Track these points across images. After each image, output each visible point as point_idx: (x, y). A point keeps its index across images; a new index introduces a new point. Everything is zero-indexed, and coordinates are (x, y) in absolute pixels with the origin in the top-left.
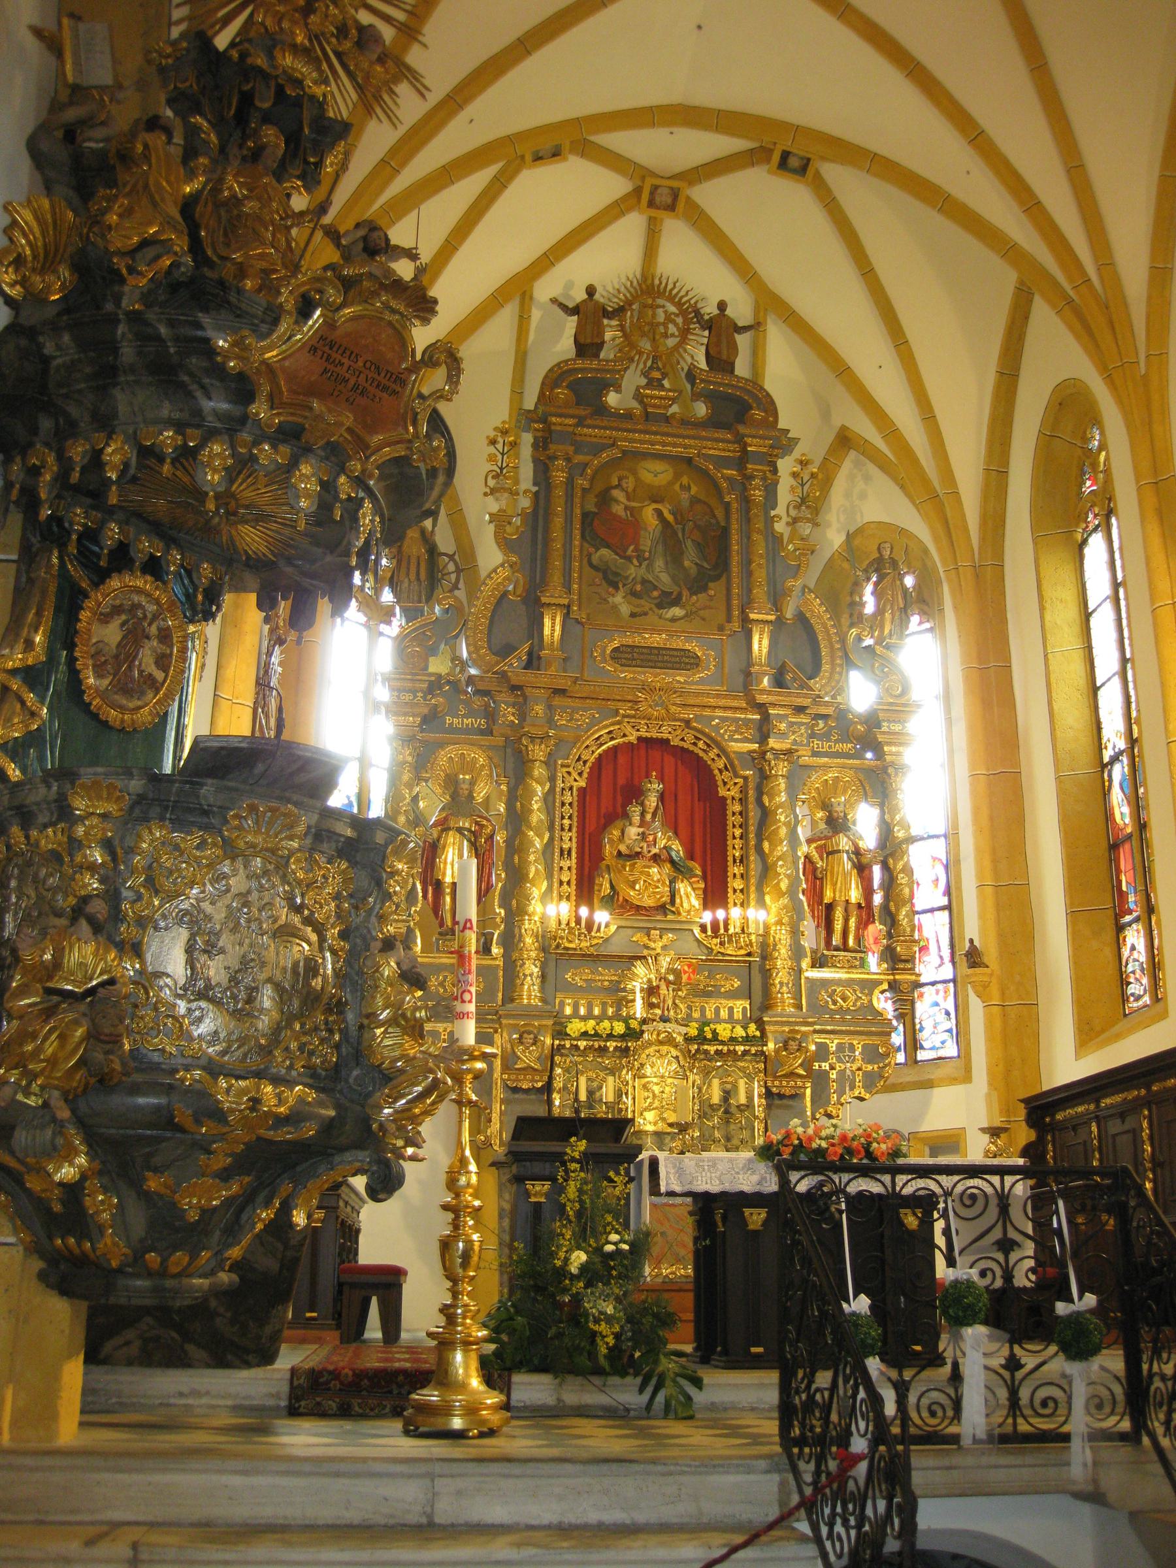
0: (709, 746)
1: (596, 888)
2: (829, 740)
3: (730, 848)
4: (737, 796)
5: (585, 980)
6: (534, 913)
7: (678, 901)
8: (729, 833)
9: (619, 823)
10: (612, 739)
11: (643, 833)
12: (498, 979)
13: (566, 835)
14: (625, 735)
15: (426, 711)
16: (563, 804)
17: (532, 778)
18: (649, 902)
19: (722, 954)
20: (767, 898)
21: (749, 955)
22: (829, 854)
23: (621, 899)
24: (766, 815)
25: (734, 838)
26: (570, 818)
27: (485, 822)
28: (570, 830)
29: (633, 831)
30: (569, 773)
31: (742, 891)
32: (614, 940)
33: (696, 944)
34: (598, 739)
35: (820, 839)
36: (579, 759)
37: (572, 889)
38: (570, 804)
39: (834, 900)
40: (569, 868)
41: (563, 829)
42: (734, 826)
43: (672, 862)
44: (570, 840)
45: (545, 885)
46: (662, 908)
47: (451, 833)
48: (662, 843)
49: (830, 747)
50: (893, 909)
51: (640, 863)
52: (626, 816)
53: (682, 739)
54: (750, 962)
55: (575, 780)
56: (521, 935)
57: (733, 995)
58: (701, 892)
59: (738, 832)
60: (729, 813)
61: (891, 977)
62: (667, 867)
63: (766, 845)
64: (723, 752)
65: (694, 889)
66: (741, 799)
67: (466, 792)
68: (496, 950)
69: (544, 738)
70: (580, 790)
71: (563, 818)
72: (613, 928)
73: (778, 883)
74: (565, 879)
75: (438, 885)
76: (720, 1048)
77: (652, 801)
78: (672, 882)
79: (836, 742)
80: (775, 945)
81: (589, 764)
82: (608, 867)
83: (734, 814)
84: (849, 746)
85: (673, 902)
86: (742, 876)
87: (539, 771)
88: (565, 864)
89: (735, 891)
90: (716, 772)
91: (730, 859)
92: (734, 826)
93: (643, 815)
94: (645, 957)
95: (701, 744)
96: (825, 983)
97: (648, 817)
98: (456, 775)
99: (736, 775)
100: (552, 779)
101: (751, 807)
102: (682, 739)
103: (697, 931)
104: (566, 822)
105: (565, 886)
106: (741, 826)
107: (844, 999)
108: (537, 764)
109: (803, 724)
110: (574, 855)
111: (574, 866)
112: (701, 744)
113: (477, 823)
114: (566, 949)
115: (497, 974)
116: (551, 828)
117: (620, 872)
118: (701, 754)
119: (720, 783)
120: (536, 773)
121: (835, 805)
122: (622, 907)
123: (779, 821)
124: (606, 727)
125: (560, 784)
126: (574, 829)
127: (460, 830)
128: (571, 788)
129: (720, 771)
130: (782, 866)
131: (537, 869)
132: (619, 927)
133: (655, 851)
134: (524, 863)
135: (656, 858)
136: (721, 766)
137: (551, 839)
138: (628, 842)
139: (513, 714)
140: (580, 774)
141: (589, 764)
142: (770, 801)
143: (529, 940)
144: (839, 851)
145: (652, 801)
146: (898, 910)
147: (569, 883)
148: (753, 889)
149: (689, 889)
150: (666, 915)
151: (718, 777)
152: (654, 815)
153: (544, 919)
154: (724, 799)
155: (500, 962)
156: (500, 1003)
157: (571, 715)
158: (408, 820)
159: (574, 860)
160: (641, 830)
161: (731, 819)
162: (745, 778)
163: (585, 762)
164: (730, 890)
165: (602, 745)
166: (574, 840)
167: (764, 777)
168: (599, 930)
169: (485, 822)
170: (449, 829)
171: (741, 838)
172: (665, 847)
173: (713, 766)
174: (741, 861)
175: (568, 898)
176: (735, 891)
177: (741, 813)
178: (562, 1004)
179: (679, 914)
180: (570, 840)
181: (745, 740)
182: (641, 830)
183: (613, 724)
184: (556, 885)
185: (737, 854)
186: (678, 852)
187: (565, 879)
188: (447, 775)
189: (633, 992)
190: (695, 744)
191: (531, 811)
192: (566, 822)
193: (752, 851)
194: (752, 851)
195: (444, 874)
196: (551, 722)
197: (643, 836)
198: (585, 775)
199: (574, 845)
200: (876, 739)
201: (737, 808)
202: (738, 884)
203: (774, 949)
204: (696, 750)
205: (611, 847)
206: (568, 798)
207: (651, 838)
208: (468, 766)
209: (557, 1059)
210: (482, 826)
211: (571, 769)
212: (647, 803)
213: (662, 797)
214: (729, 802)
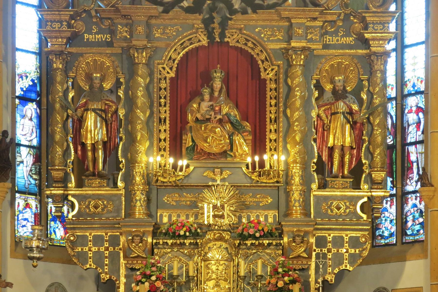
0: (254, 44)
1: (184, 142)
2: (337, 36)
3: (268, 113)
4: (273, 78)
5: (176, 201)
6: (140, 162)
7: (234, 148)
8: (268, 103)
9: (198, 99)
10: (191, 44)
11: (212, 105)
12: (122, 203)
13: (162, 109)
14: (199, 41)
15: (68, 34)
16: (160, 89)
17: (138, 75)
18: (215, 150)
19: (262, 182)
20: (289, 146)
21: (277, 182)
22: (332, 114)
23: (199, 148)
24: (290, 89)
25: (271, 106)
26: (165, 98)
27: (111, 104)
28: (165, 106)
29: (205, 105)
30: (164, 68)
31: (275, 140)
32: (192, 176)
33: (244, 176)
34: (182, 44)
35: (326, 105)
36: (170, 58)
37: (167, 144)
38: (165, 89)
39: (334, 145)
40: (165, 131)
41: (160, 105)
42: (271, 98)
43: (232, 123)
44: (165, 112)
45: (148, 144)
46: (224, 154)
47: (89, 112)
48: (225, 110)
49: (338, 40)
50: (371, 150)
51: (210, 126)
52: (201, 95)
53: (238, 41)
54: (278, 187)
55: (168, 73)
56: (133, 175)
57: (267, 207)
58: (250, 142)
59: (273, 102)
60: (268, 89)
61: (370, 194)
62: (228, 127)
63: (288, 111)
64: (264, 49)
65: (245, 140)
66: (276, 80)
67: (98, 85)
68: (120, 184)
69: (145, 48)
70: (171, 79)
71: (160, 98)
72: (191, 168)
73: (295, 137)
74: (163, 137)
75: (84, 145)
76: (254, 242)
77: (217, 84)
78: (231, 136)
79: (342, 36)
80: (292, 176)
81: (176, 62)
82: (191, 127)
83: (271, 90)
84: (351, 39)
85: (231, 150)
86: (276, 130)
87: (142, 70)
88: (162, 128)
89: (271, 140)
90: (260, 62)
91: (268, 120)
92: (271, 98)
93: (212, 94)
94: (209, 186)
95: (250, 44)
96: (326, 198)
97: (216, 94)
98: (92, 74)
99: (273, 65)
100: (151, 74)
101: (281, 85)
102: (238, 41)
103: (244, 169)
104: (162, 101)
105: (163, 142)
106: (275, 98)
107: (338, 208)
108: (141, 66)
109: (317, 27)
110: (168, 122)
111: (168, 129)
112: (250, 44)
113: (106, 104)
114: (164, 182)
115: (121, 199)
116: (151, 107)
117: (198, 130)
118: (250, 51)
119: (262, 70)
120: (140, 72)
121: (337, 82)
122: (199, 153)
123: (297, 95)
124: (186, 36)
125: (157, 76)
126: (168, 105)
127: (94, 110)
128: (165, 78)
129: (263, 62)
130: (297, 126)
131: (142, 135)
132: (195, 168)
133: (219, 117)
134: (134, 128)
135: (220, 121)
136: (263, 58)
137: (152, 113)
138: (202, 112)
139: (126, 32)
140: (171, 69)
141: (176, 62)
142: (292, 82)
143: (138, 179)
144: (337, 113)
145: (217, 84)
146: (374, 151)
147: (165, 140)
148: (281, 139)
149: (242, 141)
150: (226, 157)
151: (261, 66)
152: (220, 92)
153: (148, 164)
154: (265, 80)
155: (123, 192)
156: (123, 217)
157: (164, 29)
158: (62, 106)
159: (168, 125)
160: (211, 103)
161: (269, 94)
162: (279, 66)
163: (174, 61)
164: (268, 140)
165: (184, 48)
166: (168, 112)
167: (290, 65)
168: (181, 170)
169: (111, 104)
170: (87, 110)
171: (275, 106)
172: (226, 114)
173: (258, 59)
174: (275, 121)
175: (165, 150)
176: (271, 140)
177: (276, 89)
178: (161, 216)
179: (235, 156)
180: (165, 112)
181: (279, 40)
182: (211, 103)
183: (191, 34)
184: (155, 143)
185: (273, 117)
186: (236, 116)
187: (163, 137)
188: (86, 74)
189: (202, 208)
190: (246, 44)
191: (137, 97)
192: (162, 101)
193: (281, 115)
194: (281, 115)
195: (86, 139)
196: (149, 36)
197: (212, 108)
198: (174, 69)
199: (168, 115)
200: (364, 36)
201: (273, 86)
202: (273, 136)
203: (292, 179)
204: (246, 48)
205: (192, 115)
206: (163, 85)
207: (217, 109)
208: (100, 67)
209: (156, 251)
210: (110, 106)
211: (165, 66)
212: (215, 85)
213: (226, 81)
214: (268, 82)
